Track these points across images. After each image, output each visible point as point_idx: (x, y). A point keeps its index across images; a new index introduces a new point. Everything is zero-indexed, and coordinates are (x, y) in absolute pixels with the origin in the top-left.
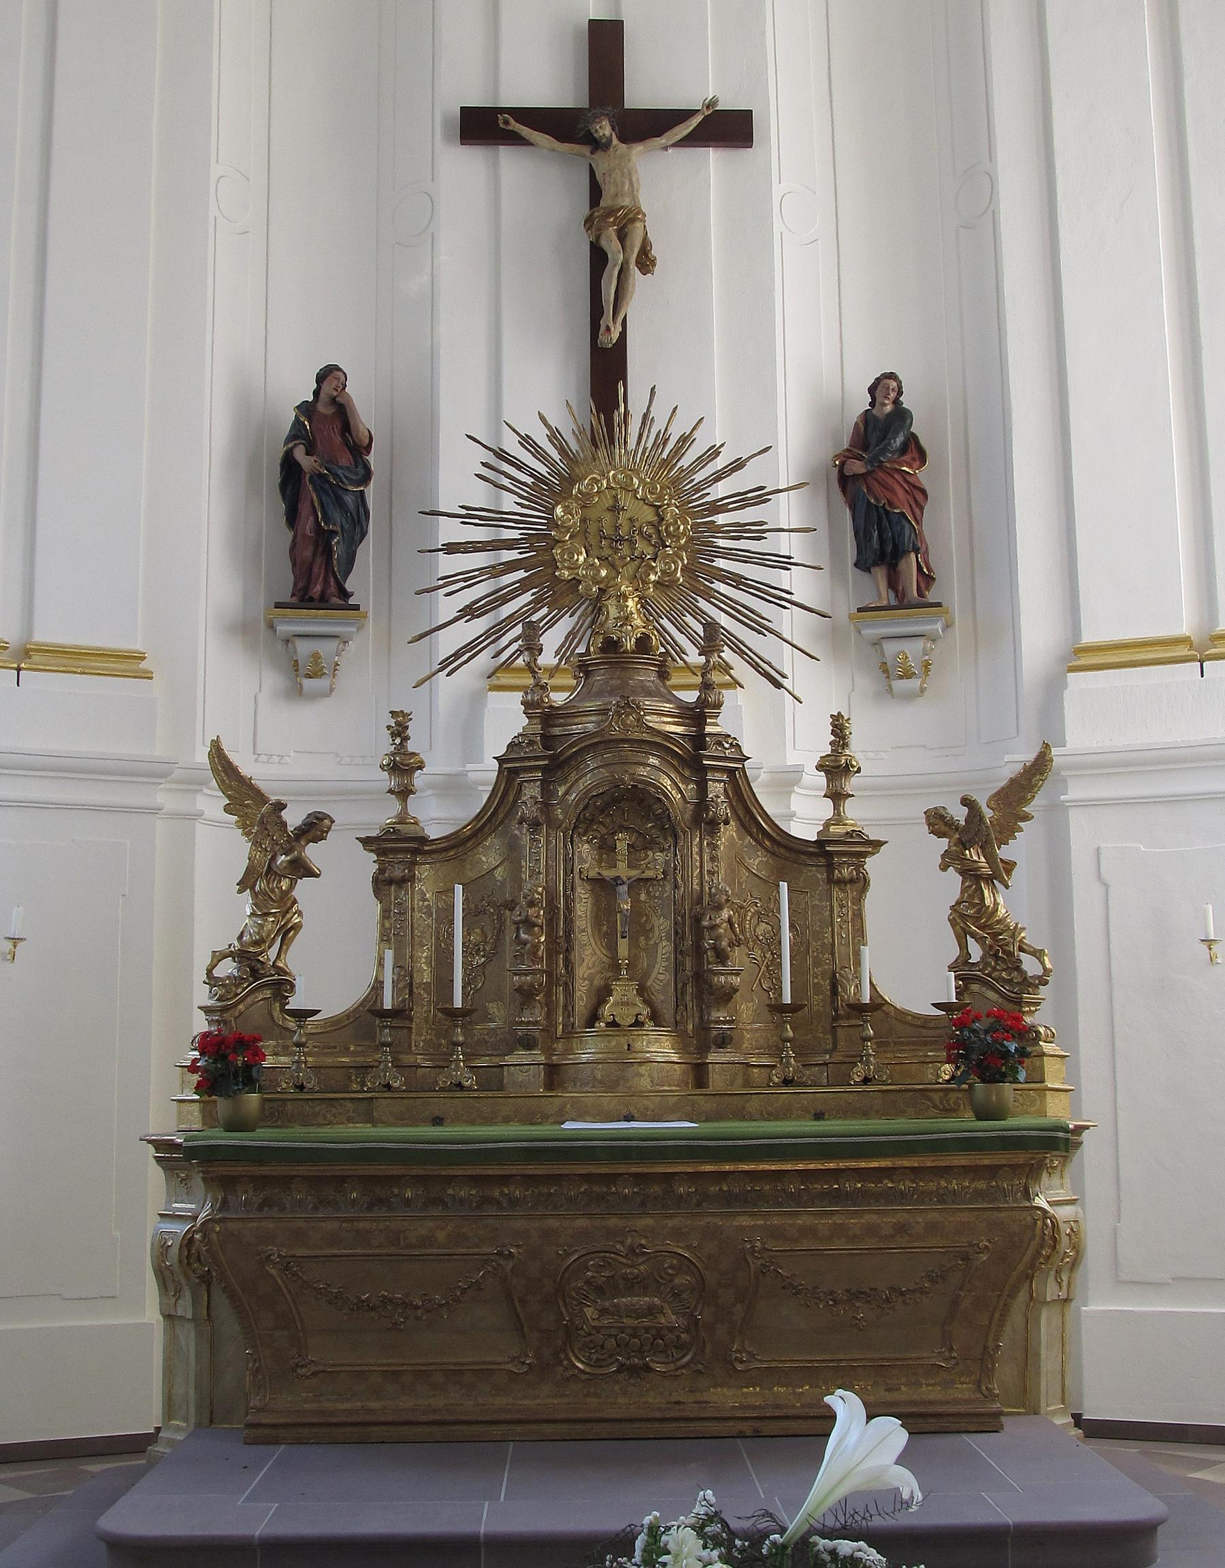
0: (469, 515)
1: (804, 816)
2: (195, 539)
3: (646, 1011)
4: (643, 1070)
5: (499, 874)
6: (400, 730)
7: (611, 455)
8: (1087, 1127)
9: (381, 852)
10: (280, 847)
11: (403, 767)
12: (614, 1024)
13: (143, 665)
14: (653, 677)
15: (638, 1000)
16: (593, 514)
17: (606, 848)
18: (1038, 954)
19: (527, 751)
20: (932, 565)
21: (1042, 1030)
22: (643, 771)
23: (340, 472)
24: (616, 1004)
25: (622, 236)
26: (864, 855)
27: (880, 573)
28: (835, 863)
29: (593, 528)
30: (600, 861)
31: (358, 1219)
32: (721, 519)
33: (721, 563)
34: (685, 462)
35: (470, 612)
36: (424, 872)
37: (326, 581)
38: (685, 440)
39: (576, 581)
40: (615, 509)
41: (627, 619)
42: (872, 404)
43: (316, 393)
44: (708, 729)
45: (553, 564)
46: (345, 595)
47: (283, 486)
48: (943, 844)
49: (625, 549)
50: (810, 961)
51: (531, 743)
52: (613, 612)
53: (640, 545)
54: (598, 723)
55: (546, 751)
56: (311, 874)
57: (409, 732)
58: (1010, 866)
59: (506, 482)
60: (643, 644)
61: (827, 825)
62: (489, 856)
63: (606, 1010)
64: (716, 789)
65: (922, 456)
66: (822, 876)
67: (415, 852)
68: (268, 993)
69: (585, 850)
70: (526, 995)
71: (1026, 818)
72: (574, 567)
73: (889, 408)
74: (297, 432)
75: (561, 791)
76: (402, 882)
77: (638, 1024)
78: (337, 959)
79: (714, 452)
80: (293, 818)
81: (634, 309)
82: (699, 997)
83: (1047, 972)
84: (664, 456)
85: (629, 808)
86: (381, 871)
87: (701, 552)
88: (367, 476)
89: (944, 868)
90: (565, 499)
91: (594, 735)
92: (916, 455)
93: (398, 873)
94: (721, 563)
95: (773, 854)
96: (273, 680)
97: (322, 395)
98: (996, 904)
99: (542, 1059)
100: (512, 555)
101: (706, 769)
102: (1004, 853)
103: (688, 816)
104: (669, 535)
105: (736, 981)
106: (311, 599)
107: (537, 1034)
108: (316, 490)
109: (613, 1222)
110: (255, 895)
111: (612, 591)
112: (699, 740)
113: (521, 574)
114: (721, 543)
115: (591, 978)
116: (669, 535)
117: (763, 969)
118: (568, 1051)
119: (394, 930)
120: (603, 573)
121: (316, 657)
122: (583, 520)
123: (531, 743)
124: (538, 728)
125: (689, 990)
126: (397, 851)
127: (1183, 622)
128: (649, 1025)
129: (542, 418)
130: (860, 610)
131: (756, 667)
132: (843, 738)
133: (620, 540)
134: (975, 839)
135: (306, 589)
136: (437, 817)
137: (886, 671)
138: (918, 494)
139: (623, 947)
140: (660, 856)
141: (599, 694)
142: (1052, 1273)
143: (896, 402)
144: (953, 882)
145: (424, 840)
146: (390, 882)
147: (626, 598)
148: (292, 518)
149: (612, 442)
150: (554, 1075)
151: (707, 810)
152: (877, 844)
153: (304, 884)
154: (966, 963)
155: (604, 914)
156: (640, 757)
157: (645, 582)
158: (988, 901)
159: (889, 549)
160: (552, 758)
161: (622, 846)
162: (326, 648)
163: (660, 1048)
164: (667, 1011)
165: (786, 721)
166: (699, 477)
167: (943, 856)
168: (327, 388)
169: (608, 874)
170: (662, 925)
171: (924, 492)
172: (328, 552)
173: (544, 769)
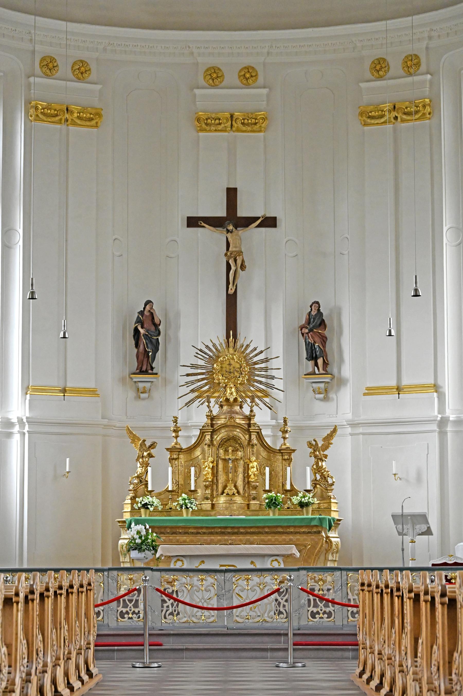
0: (193, 366)
2: (109, 353)
3: (236, 491)
4: (235, 505)
5: (200, 457)
6: (176, 421)
7: (228, 350)
8: (341, 520)
9: (170, 452)
10: (147, 450)
12: (228, 494)
13: (96, 393)
14: (239, 407)
15: (234, 488)
16: (224, 366)
17: (226, 451)
18: (332, 478)
19: (207, 428)
20: (328, 359)
21: (332, 496)
22: (235, 433)
23: (152, 333)
24: (229, 489)
25: (235, 261)
26: (291, 453)
27: (311, 363)
28: (286, 454)
29: (224, 369)
30: (225, 454)
31: (169, 537)
32: (256, 366)
33: (256, 378)
34: (248, 351)
35: (192, 391)
36: (181, 456)
37: (147, 365)
38: (248, 346)
39: (219, 383)
40: (230, 364)
41: (231, 394)
42: (311, 310)
43: (144, 308)
44: (252, 422)
45: (214, 379)
46: (152, 368)
47: (134, 336)
48: (311, 450)
49: (232, 375)
50: (277, 479)
51: (208, 426)
52: (229, 391)
53: (236, 374)
54: (225, 421)
55: (212, 426)
56: (152, 456)
57: (178, 422)
58: (326, 456)
59: (202, 357)
60: (235, 400)
61: (282, 445)
62: (198, 452)
63: (226, 491)
64: (254, 437)
65: (325, 326)
66: (280, 458)
67: (179, 452)
68: (144, 486)
69: (221, 451)
70: (206, 487)
71: (331, 444)
72: (219, 380)
73: (316, 312)
74: (139, 321)
75: (215, 437)
76: (176, 459)
77: (234, 494)
79: (255, 349)
80: (148, 444)
81: (239, 282)
82: (249, 488)
83: (334, 482)
84: (242, 350)
86: (171, 456)
87: (251, 375)
88: (159, 334)
89: (311, 456)
90: (217, 362)
91: (223, 424)
92: (323, 326)
93: (175, 457)
94: (256, 378)
95: (269, 452)
97: (146, 309)
98: (322, 466)
99: (210, 502)
100: (204, 376)
101: (251, 432)
102: (326, 453)
103: (246, 443)
104: (243, 371)
105: (258, 484)
106: (143, 372)
107: (209, 497)
108: (145, 339)
109: (226, 538)
110: (140, 462)
111: (228, 386)
112: (249, 425)
113: (206, 381)
114: (256, 373)
115: (222, 483)
116: (243, 371)
118: (217, 501)
120: (226, 381)
121: (144, 388)
122: (222, 367)
123: (208, 426)
124: (210, 422)
125: (246, 486)
128: (237, 494)
129: (211, 341)
130: (305, 375)
131: (265, 404)
132: (286, 423)
133: (230, 373)
135: (141, 368)
137: (314, 392)
138: (324, 340)
139: (230, 475)
140: (240, 453)
141: (225, 413)
142: (331, 553)
143: (319, 310)
144: (313, 460)
145: (182, 449)
146: (173, 459)
147: (231, 388)
148: (137, 345)
149: (229, 347)
150: (213, 506)
151: (251, 442)
152: (294, 451)
153: (151, 459)
154: (316, 480)
155: (226, 468)
156: (235, 429)
157: (237, 383)
158: (320, 465)
159: (314, 355)
160: (213, 430)
161: (230, 451)
162: (148, 385)
164: (241, 491)
166: (251, 355)
167: (310, 453)
168: (148, 307)
169: (227, 457)
170: (241, 470)
171: (326, 338)
172: (148, 357)
173: (211, 432)
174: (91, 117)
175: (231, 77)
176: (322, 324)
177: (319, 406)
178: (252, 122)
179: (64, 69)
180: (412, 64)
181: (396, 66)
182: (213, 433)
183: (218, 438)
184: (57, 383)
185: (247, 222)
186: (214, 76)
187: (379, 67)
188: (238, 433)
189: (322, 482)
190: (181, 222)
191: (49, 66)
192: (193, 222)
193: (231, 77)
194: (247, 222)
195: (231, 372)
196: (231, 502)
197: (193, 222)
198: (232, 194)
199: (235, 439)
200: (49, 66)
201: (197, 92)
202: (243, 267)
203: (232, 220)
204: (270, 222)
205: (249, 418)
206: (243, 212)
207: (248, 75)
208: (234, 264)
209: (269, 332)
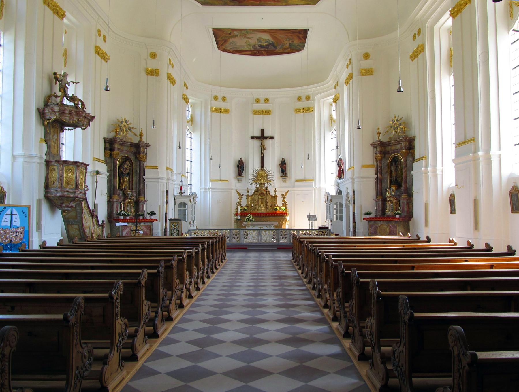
1: (273, 194)
2: (231, 171)
10: (241, 196)
11: (248, 191)
55: (257, 190)
62: (253, 197)
78: (244, 202)
85: (262, 194)
96: (237, 181)
117: (270, 204)
119: (247, 201)
126: (248, 196)
127: (302, 178)
134: (283, 195)
136: (250, 194)
138: (285, 167)
163: (264, 209)
165: (276, 186)
174: (227, 111)
175: (262, 101)
176: (285, 164)
177: (284, 184)
178: (268, 112)
179: (220, 99)
180: (308, 98)
181: (304, 98)
182: (257, 191)
183: (259, 192)
184: (218, 179)
185: (266, 138)
186: (258, 101)
187: (300, 99)
188: (263, 192)
189: (285, 204)
190: (249, 138)
191: (216, 98)
192: (252, 138)
193: (262, 101)
194: (266, 138)
195: (262, 176)
196: (262, 209)
197: (252, 138)
198: (262, 131)
199: (263, 193)
200: (216, 98)
201: (254, 105)
202: (265, 149)
203: (262, 137)
204: (272, 138)
205: (266, 188)
206: (265, 135)
207: (266, 100)
208: (262, 148)
209: (272, 166)
